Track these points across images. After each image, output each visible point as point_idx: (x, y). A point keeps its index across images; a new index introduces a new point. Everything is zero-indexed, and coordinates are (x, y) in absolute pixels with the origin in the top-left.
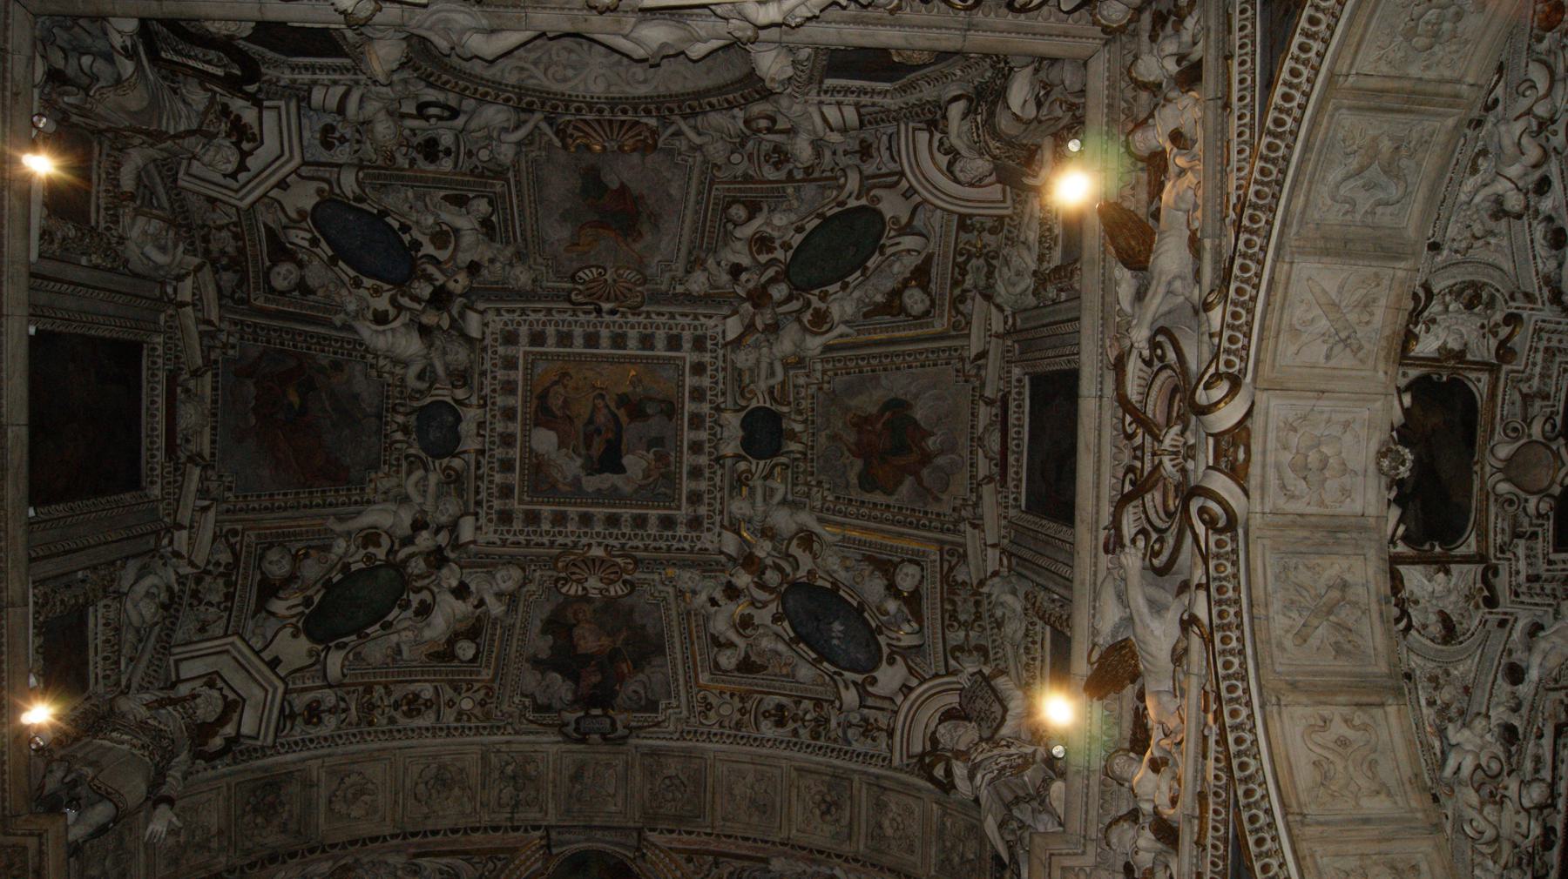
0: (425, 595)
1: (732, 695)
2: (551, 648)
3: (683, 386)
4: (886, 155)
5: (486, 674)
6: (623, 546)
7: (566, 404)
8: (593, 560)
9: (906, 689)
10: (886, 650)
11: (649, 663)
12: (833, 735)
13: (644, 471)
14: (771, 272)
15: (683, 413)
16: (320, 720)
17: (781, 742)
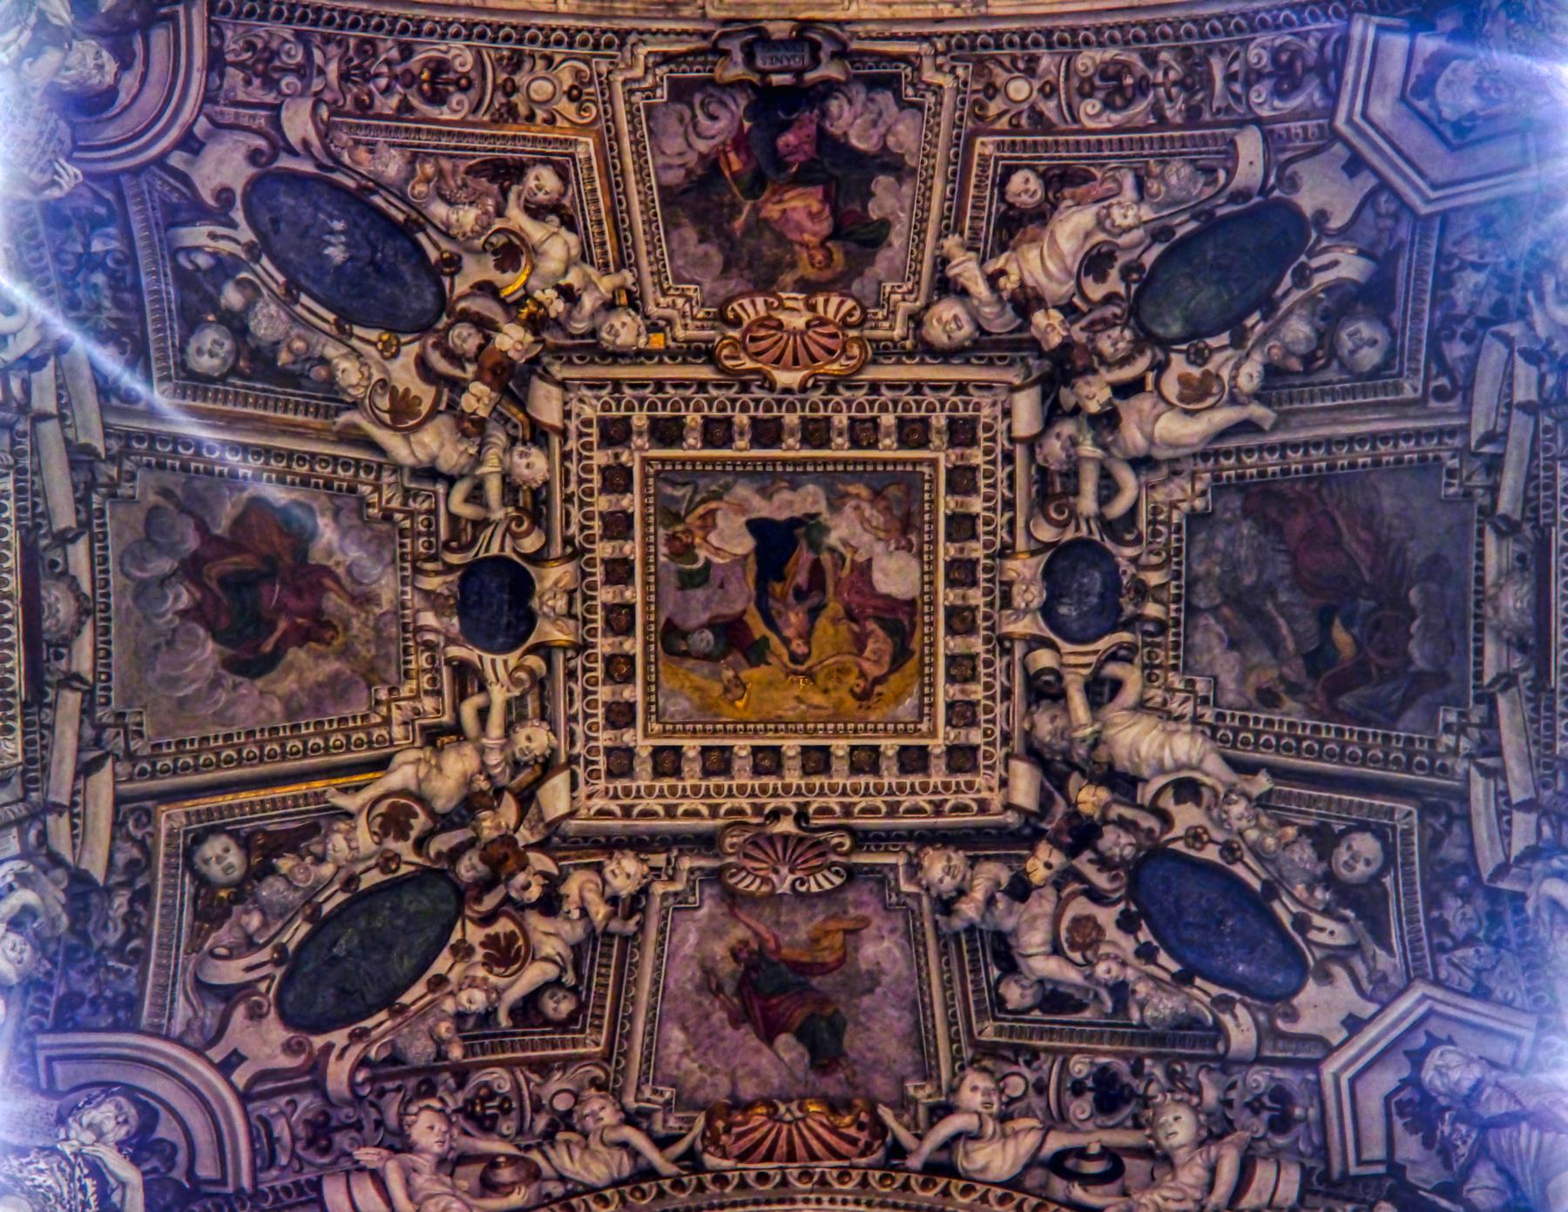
0: (1096, 291)
1: (531, 117)
2: (871, 195)
3: (647, 684)
4: (281, 1129)
5: (985, 146)
7: (860, 642)
8: (796, 361)
11: (689, 172)
12: (333, 50)
13: (714, 526)
15: (646, 633)
16: (1275, 59)
17: (431, 33)
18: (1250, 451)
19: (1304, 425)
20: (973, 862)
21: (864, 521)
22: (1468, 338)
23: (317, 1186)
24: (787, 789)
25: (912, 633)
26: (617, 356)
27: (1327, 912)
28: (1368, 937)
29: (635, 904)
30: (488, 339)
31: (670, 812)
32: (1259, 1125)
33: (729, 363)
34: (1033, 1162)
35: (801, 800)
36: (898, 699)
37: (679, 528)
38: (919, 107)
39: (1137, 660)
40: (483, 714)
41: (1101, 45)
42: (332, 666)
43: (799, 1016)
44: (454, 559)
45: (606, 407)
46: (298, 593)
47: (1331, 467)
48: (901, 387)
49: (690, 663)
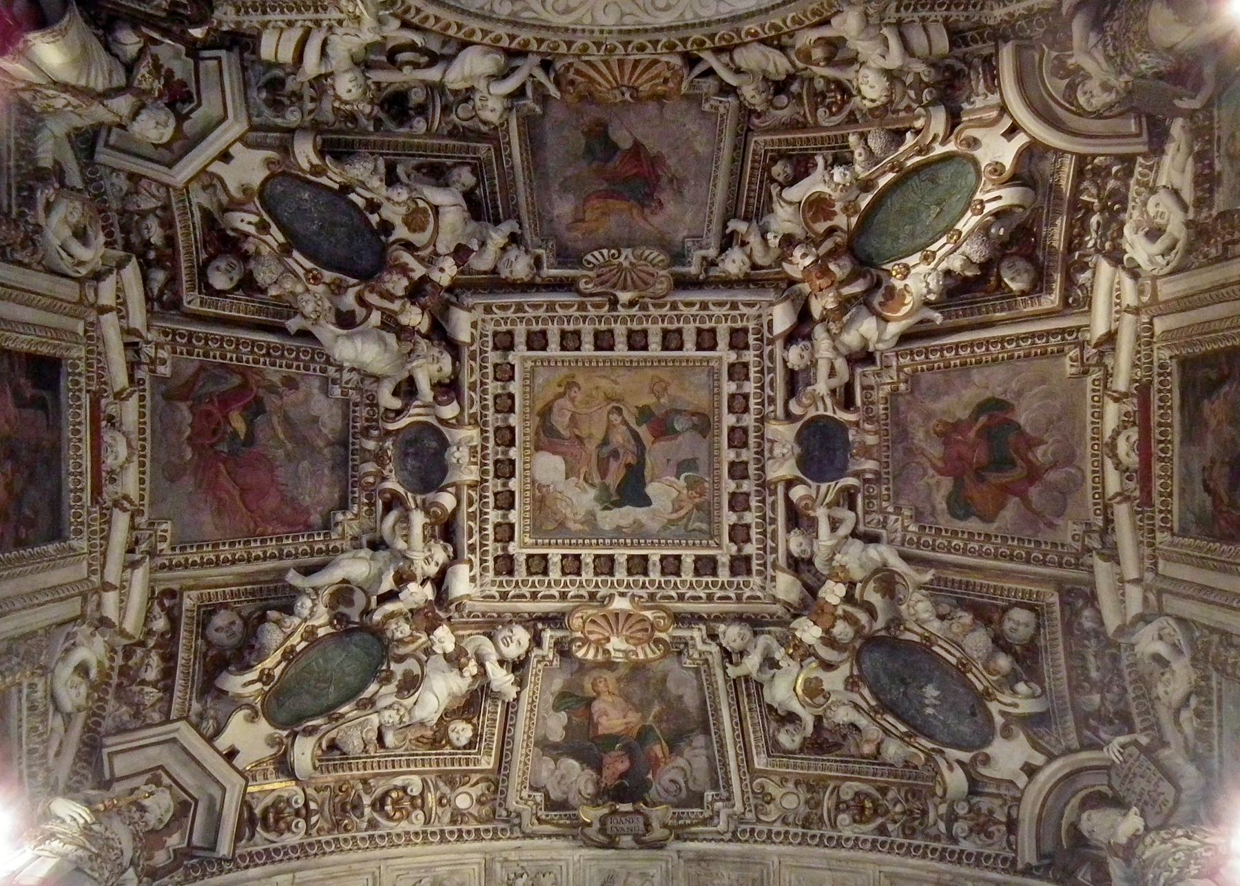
0: (412, 665)
2: (565, 728)
5: (487, 763)
6: (652, 597)
7: (574, 421)
8: (617, 615)
9: (1031, 771)
10: (999, 720)
14: (828, 245)
15: (720, 428)
18: (305, 553)
19: (266, 572)
20: (494, 271)
21: (571, 505)
22: (150, 633)
23: (953, 44)
24: (624, 321)
26: (740, 618)
27: (246, 235)
28: (216, 216)
29: (728, 241)
30: (827, 631)
31: (704, 306)
32: (291, 85)
34: (450, 59)
35: (615, 314)
36: (548, 381)
37: (697, 500)
38: (531, 787)
39: (382, 410)
40: (832, 373)
41: (407, 833)
42: (938, 406)
43: (616, 161)
44: (851, 481)
45: (747, 584)
46: (960, 457)
47: (247, 543)
48: (545, 597)
49: (690, 408)
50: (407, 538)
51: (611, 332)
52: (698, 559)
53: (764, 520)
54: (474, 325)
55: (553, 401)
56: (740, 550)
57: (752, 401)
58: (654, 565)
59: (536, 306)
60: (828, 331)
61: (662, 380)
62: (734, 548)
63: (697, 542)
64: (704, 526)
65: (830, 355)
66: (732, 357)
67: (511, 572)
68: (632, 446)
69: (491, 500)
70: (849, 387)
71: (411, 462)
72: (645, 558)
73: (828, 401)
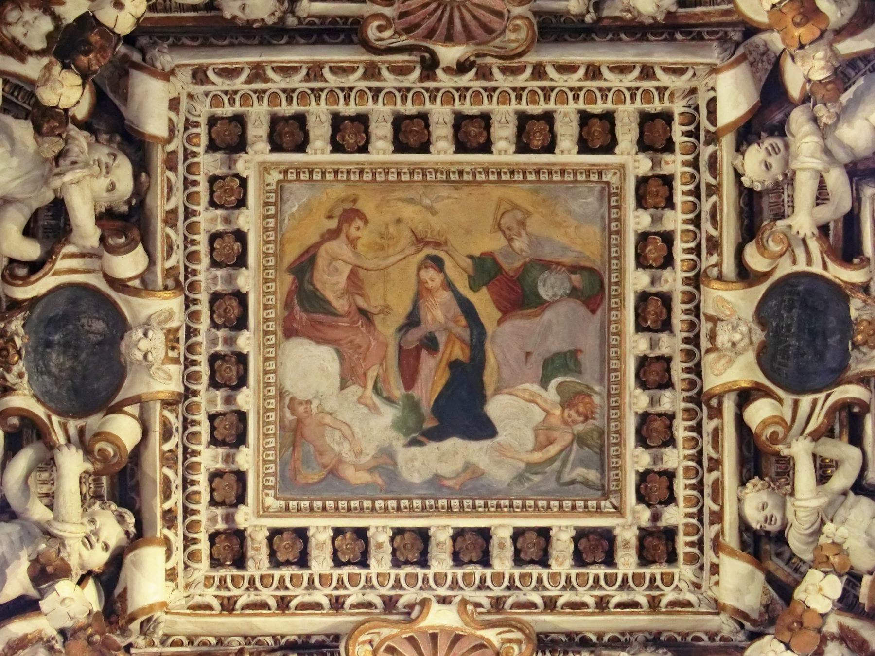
6: (498, 604)
7: (355, 282)
8: (434, 637)
13: (536, 430)
15: (621, 296)
21: (349, 437)
24: (449, 98)
25: (289, 293)
31: (594, 72)
33: (516, 635)
35: (431, 85)
36: (307, 209)
37: (580, 428)
40: (822, 195)
44: (853, 392)
45: (668, 580)
48: (304, 607)
49: (567, 259)
50: (51, 500)
51: (424, 117)
52: (581, 535)
53: (700, 463)
54: (174, 104)
55: (318, 245)
56: (656, 517)
57: (679, 246)
58: (502, 546)
59: (286, 70)
60: (815, 120)
61: (516, 207)
62: (645, 514)
63: (580, 504)
64: (593, 475)
65: (817, 163)
66: (643, 165)
67: (240, 562)
68: (461, 329)
69: (204, 429)
70: (852, 221)
71: (55, 358)
72: (485, 534)
73: (814, 246)
